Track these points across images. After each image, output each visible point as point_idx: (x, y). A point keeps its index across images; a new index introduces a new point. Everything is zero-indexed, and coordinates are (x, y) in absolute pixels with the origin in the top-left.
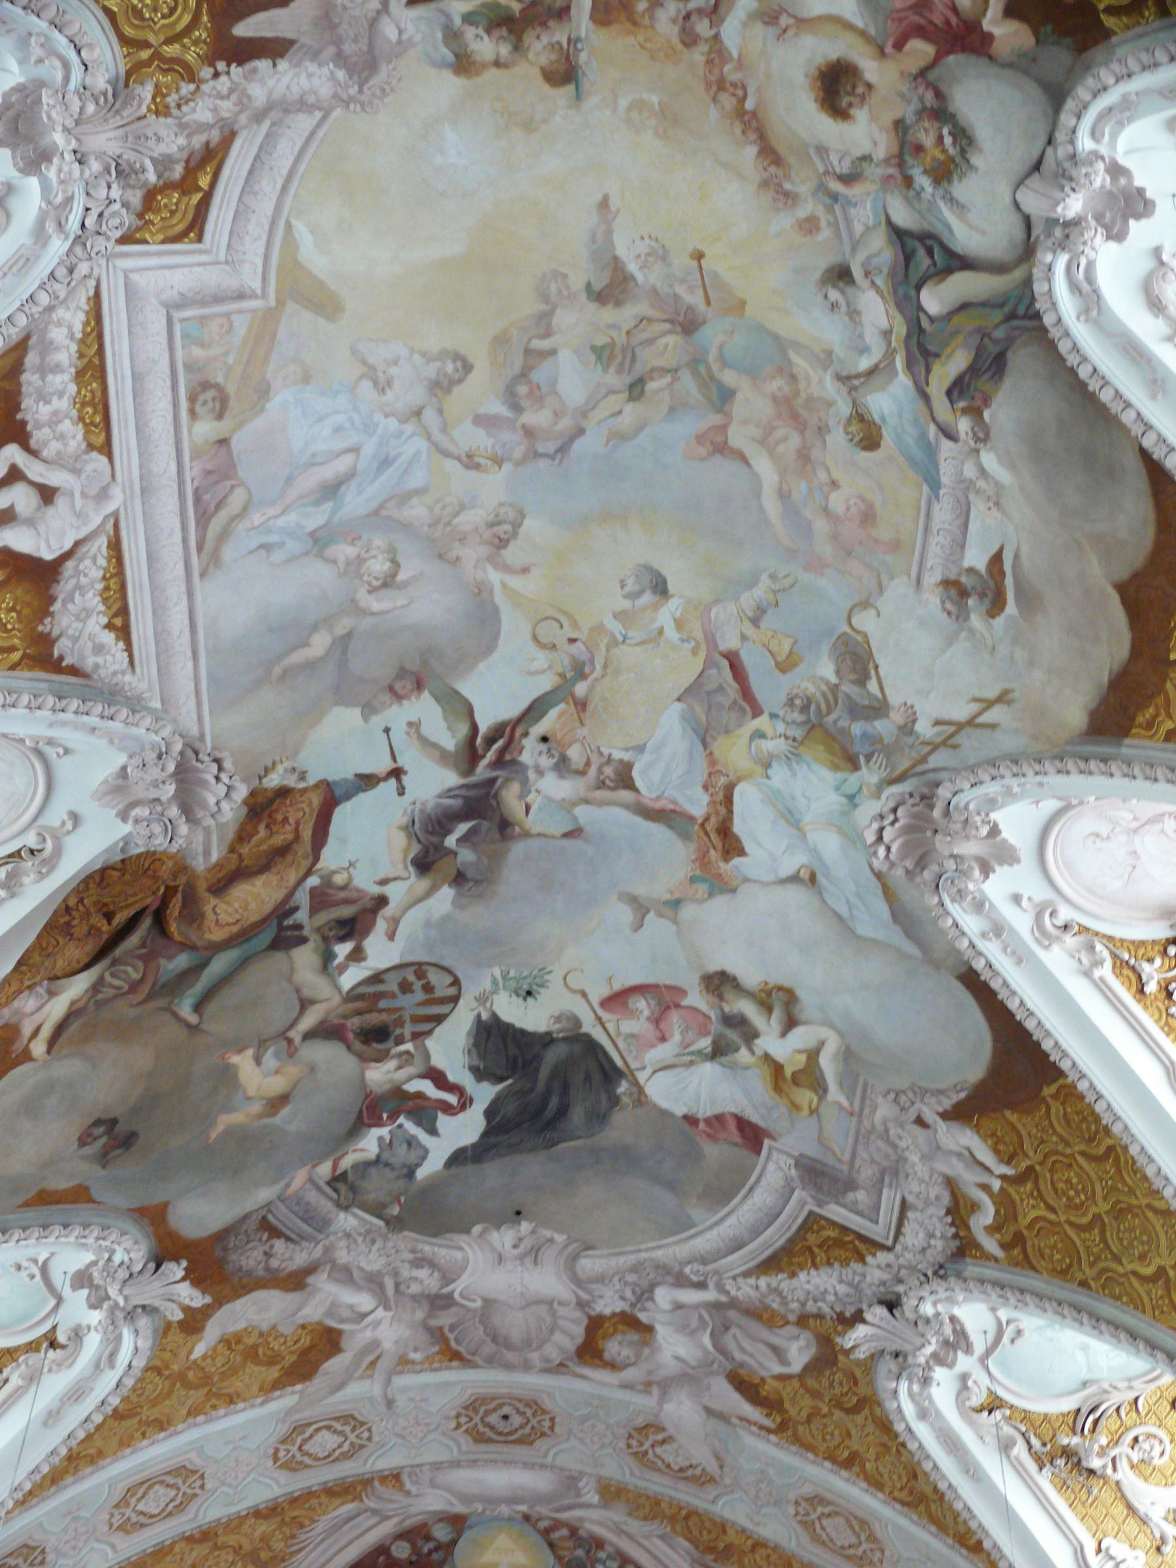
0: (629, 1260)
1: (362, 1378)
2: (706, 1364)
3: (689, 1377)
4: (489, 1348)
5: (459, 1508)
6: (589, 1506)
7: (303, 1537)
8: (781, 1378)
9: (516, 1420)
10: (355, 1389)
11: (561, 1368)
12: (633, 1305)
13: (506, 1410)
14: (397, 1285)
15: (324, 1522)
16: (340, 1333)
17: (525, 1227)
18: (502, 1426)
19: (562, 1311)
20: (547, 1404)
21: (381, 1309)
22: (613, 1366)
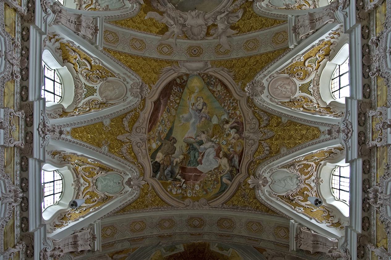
0: (212, 13)
1: (171, 38)
2: (226, 28)
3: (224, 32)
4: (192, 36)
5: (188, 72)
6: (210, 68)
7: (162, 70)
8: (238, 21)
9: (197, 51)
10: (170, 40)
11: (203, 39)
12: (214, 22)
13: (195, 49)
14: (177, 20)
15: (165, 70)
16: (168, 27)
17: (197, 11)
18: (195, 53)
19: (203, 27)
20: (202, 47)
21: (174, 25)
22: (212, 35)
